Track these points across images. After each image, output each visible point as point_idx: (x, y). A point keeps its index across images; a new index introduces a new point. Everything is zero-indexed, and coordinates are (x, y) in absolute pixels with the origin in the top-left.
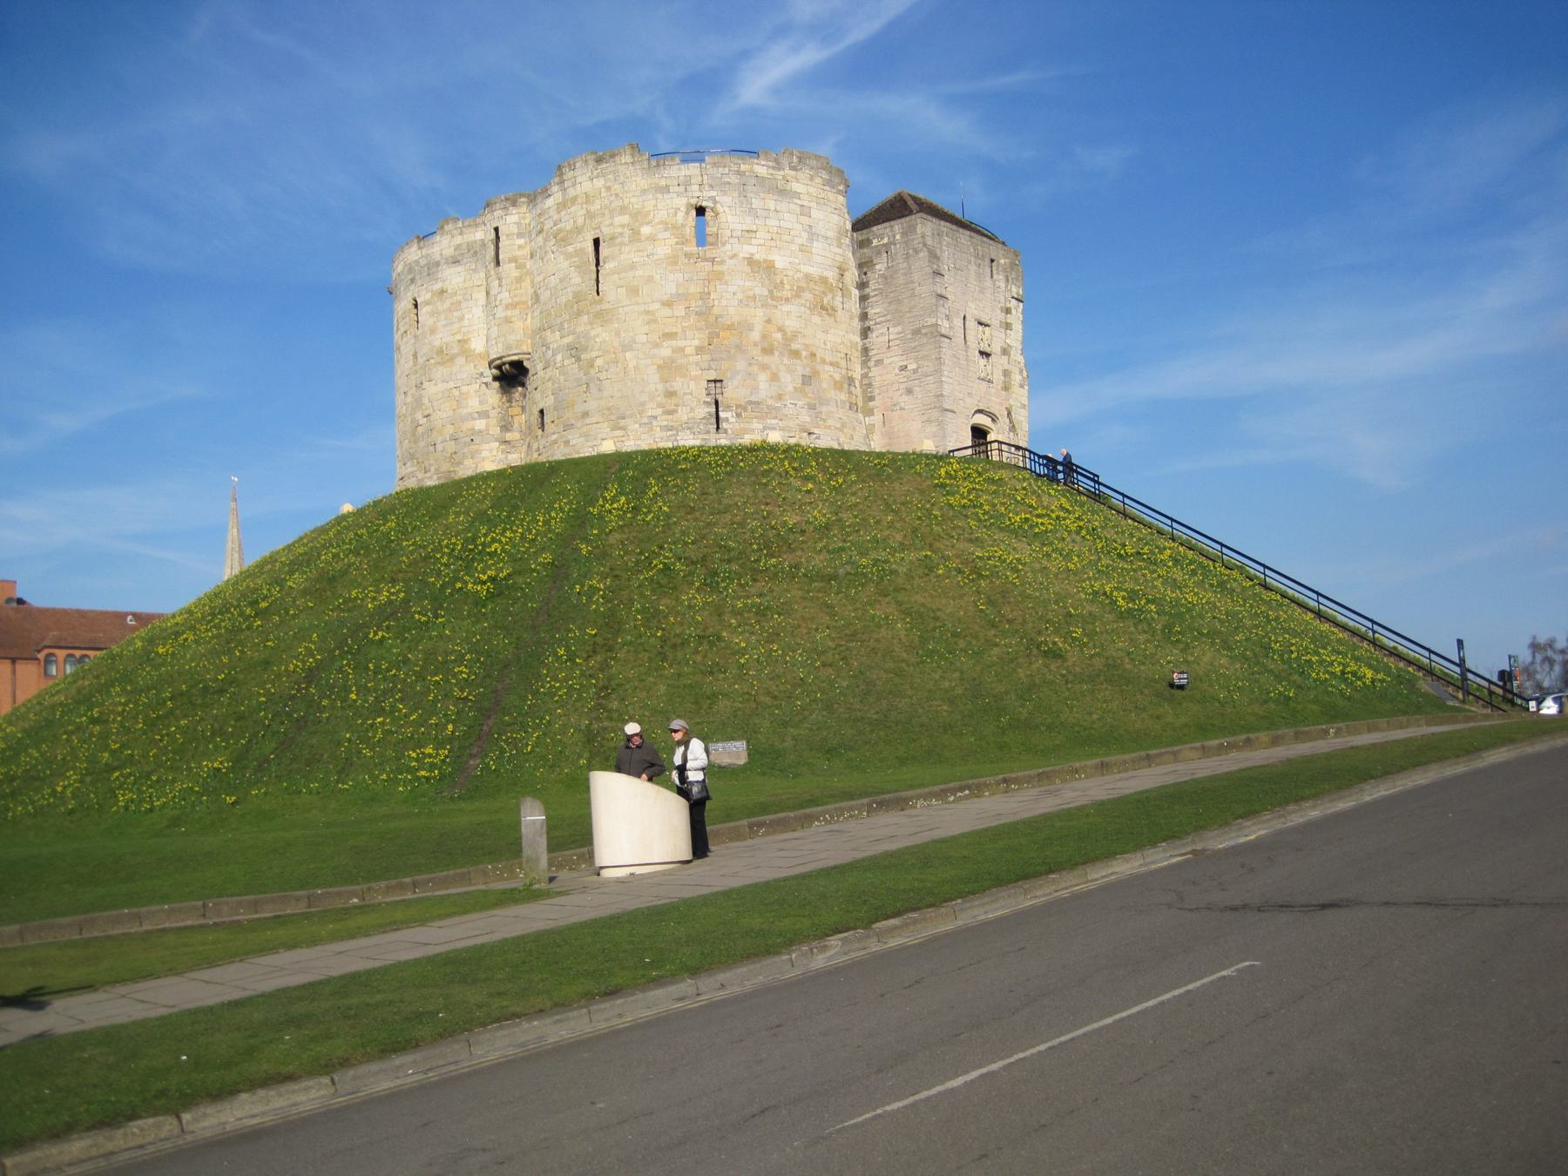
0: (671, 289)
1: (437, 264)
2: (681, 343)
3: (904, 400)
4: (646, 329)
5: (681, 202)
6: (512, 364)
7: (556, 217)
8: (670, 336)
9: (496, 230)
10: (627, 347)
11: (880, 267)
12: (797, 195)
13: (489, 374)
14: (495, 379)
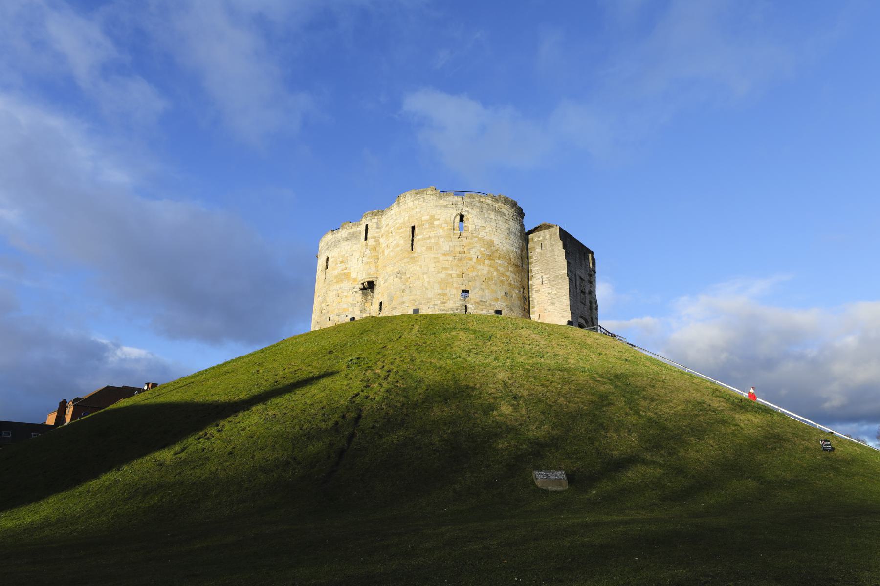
1: (339, 241)
2: (450, 272)
3: (550, 308)
4: (433, 265)
5: (455, 212)
9: (367, 226)
10: (424, 274)
11: (538, 250)
12: (504, 214)
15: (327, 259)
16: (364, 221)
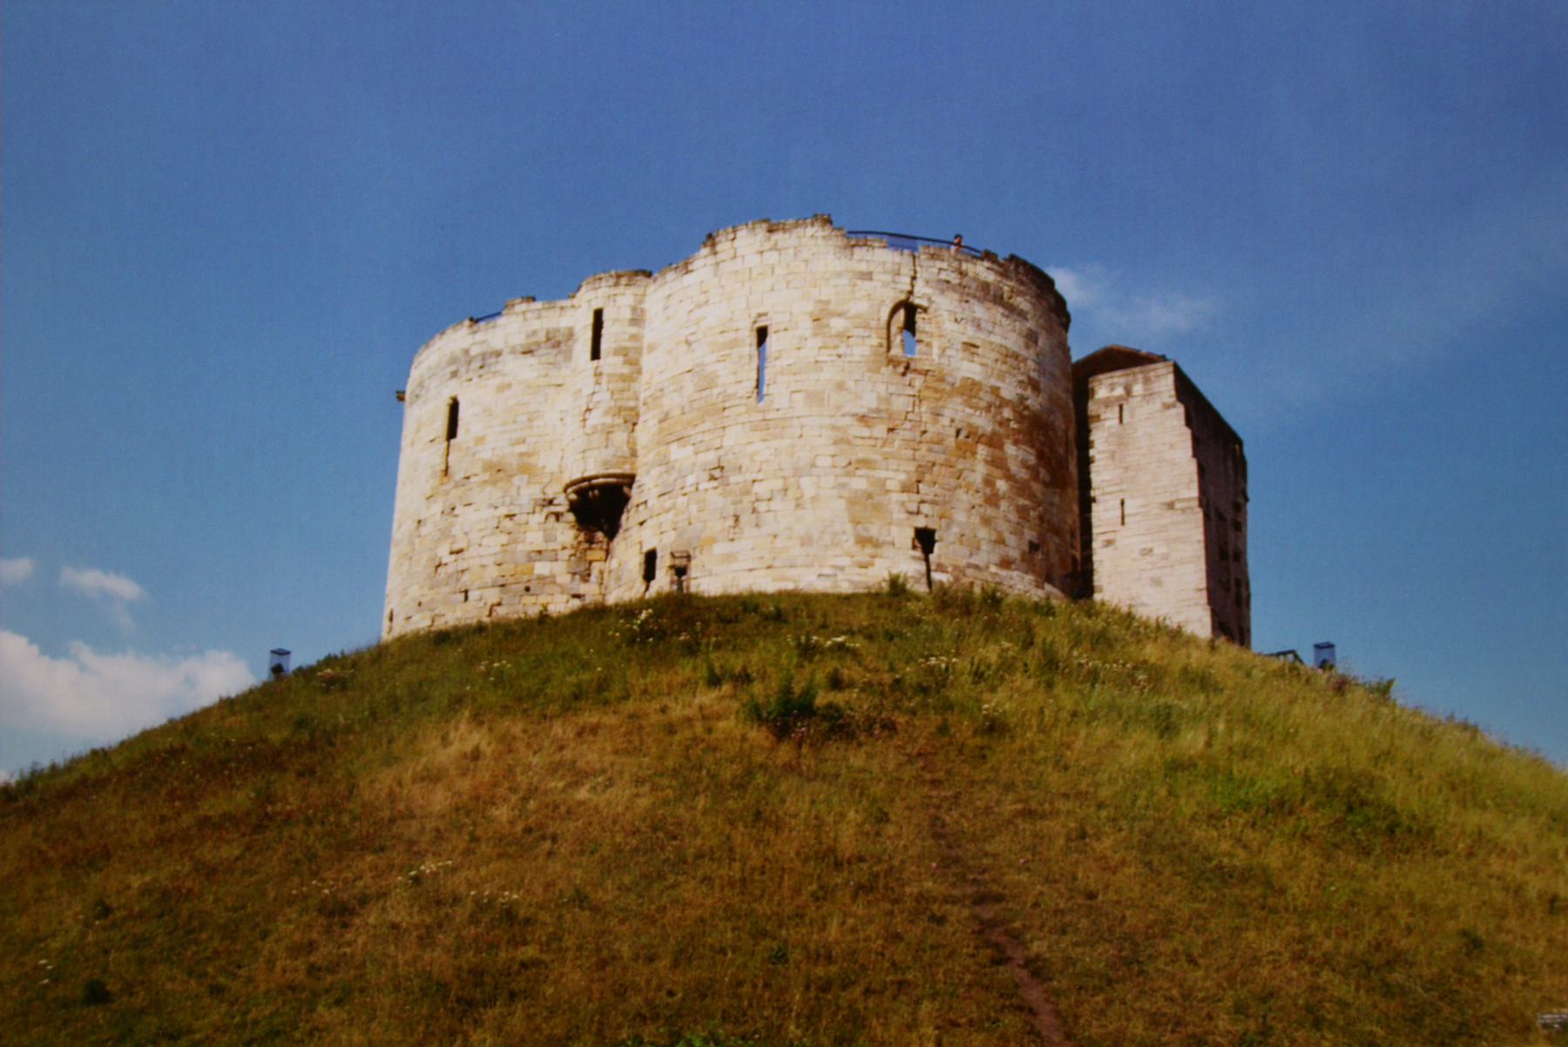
0: (869, 402)
2: (881, 474)
4: (832, 450)
6: (602, 487)
7: (702, 298)
8: (866, 463)
9: (598, 315)
10: (798, 472)
13: (562, 504)
14: (573, 507)
15: (454, 408)
16: (589, 298)
